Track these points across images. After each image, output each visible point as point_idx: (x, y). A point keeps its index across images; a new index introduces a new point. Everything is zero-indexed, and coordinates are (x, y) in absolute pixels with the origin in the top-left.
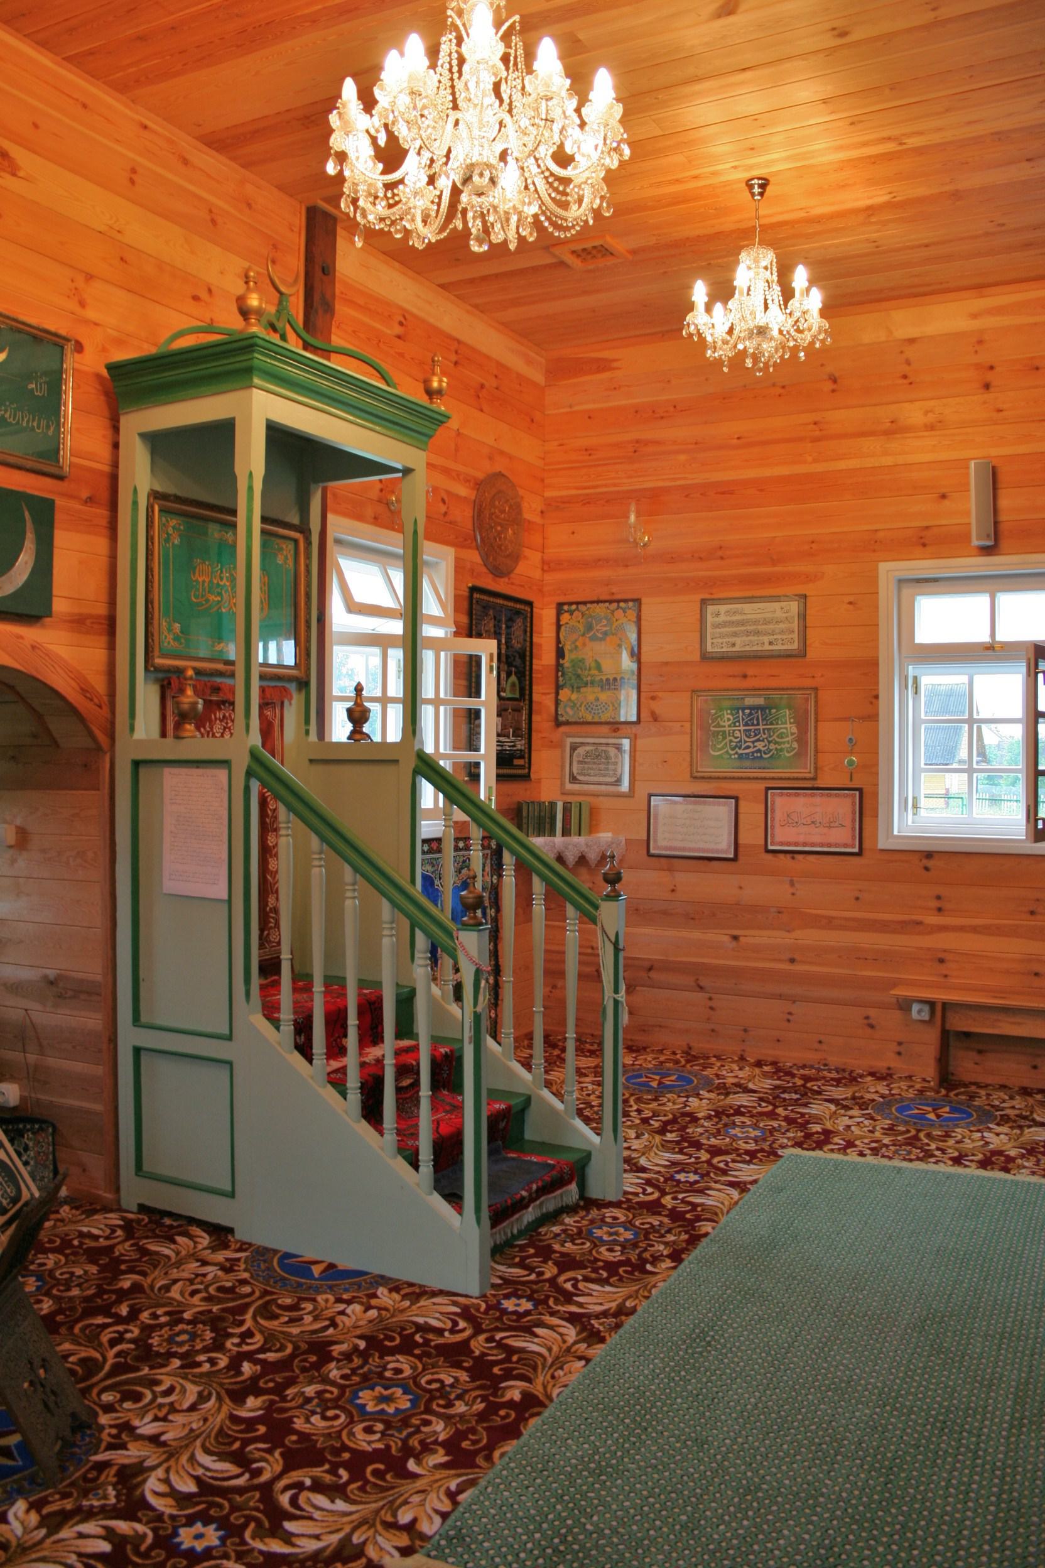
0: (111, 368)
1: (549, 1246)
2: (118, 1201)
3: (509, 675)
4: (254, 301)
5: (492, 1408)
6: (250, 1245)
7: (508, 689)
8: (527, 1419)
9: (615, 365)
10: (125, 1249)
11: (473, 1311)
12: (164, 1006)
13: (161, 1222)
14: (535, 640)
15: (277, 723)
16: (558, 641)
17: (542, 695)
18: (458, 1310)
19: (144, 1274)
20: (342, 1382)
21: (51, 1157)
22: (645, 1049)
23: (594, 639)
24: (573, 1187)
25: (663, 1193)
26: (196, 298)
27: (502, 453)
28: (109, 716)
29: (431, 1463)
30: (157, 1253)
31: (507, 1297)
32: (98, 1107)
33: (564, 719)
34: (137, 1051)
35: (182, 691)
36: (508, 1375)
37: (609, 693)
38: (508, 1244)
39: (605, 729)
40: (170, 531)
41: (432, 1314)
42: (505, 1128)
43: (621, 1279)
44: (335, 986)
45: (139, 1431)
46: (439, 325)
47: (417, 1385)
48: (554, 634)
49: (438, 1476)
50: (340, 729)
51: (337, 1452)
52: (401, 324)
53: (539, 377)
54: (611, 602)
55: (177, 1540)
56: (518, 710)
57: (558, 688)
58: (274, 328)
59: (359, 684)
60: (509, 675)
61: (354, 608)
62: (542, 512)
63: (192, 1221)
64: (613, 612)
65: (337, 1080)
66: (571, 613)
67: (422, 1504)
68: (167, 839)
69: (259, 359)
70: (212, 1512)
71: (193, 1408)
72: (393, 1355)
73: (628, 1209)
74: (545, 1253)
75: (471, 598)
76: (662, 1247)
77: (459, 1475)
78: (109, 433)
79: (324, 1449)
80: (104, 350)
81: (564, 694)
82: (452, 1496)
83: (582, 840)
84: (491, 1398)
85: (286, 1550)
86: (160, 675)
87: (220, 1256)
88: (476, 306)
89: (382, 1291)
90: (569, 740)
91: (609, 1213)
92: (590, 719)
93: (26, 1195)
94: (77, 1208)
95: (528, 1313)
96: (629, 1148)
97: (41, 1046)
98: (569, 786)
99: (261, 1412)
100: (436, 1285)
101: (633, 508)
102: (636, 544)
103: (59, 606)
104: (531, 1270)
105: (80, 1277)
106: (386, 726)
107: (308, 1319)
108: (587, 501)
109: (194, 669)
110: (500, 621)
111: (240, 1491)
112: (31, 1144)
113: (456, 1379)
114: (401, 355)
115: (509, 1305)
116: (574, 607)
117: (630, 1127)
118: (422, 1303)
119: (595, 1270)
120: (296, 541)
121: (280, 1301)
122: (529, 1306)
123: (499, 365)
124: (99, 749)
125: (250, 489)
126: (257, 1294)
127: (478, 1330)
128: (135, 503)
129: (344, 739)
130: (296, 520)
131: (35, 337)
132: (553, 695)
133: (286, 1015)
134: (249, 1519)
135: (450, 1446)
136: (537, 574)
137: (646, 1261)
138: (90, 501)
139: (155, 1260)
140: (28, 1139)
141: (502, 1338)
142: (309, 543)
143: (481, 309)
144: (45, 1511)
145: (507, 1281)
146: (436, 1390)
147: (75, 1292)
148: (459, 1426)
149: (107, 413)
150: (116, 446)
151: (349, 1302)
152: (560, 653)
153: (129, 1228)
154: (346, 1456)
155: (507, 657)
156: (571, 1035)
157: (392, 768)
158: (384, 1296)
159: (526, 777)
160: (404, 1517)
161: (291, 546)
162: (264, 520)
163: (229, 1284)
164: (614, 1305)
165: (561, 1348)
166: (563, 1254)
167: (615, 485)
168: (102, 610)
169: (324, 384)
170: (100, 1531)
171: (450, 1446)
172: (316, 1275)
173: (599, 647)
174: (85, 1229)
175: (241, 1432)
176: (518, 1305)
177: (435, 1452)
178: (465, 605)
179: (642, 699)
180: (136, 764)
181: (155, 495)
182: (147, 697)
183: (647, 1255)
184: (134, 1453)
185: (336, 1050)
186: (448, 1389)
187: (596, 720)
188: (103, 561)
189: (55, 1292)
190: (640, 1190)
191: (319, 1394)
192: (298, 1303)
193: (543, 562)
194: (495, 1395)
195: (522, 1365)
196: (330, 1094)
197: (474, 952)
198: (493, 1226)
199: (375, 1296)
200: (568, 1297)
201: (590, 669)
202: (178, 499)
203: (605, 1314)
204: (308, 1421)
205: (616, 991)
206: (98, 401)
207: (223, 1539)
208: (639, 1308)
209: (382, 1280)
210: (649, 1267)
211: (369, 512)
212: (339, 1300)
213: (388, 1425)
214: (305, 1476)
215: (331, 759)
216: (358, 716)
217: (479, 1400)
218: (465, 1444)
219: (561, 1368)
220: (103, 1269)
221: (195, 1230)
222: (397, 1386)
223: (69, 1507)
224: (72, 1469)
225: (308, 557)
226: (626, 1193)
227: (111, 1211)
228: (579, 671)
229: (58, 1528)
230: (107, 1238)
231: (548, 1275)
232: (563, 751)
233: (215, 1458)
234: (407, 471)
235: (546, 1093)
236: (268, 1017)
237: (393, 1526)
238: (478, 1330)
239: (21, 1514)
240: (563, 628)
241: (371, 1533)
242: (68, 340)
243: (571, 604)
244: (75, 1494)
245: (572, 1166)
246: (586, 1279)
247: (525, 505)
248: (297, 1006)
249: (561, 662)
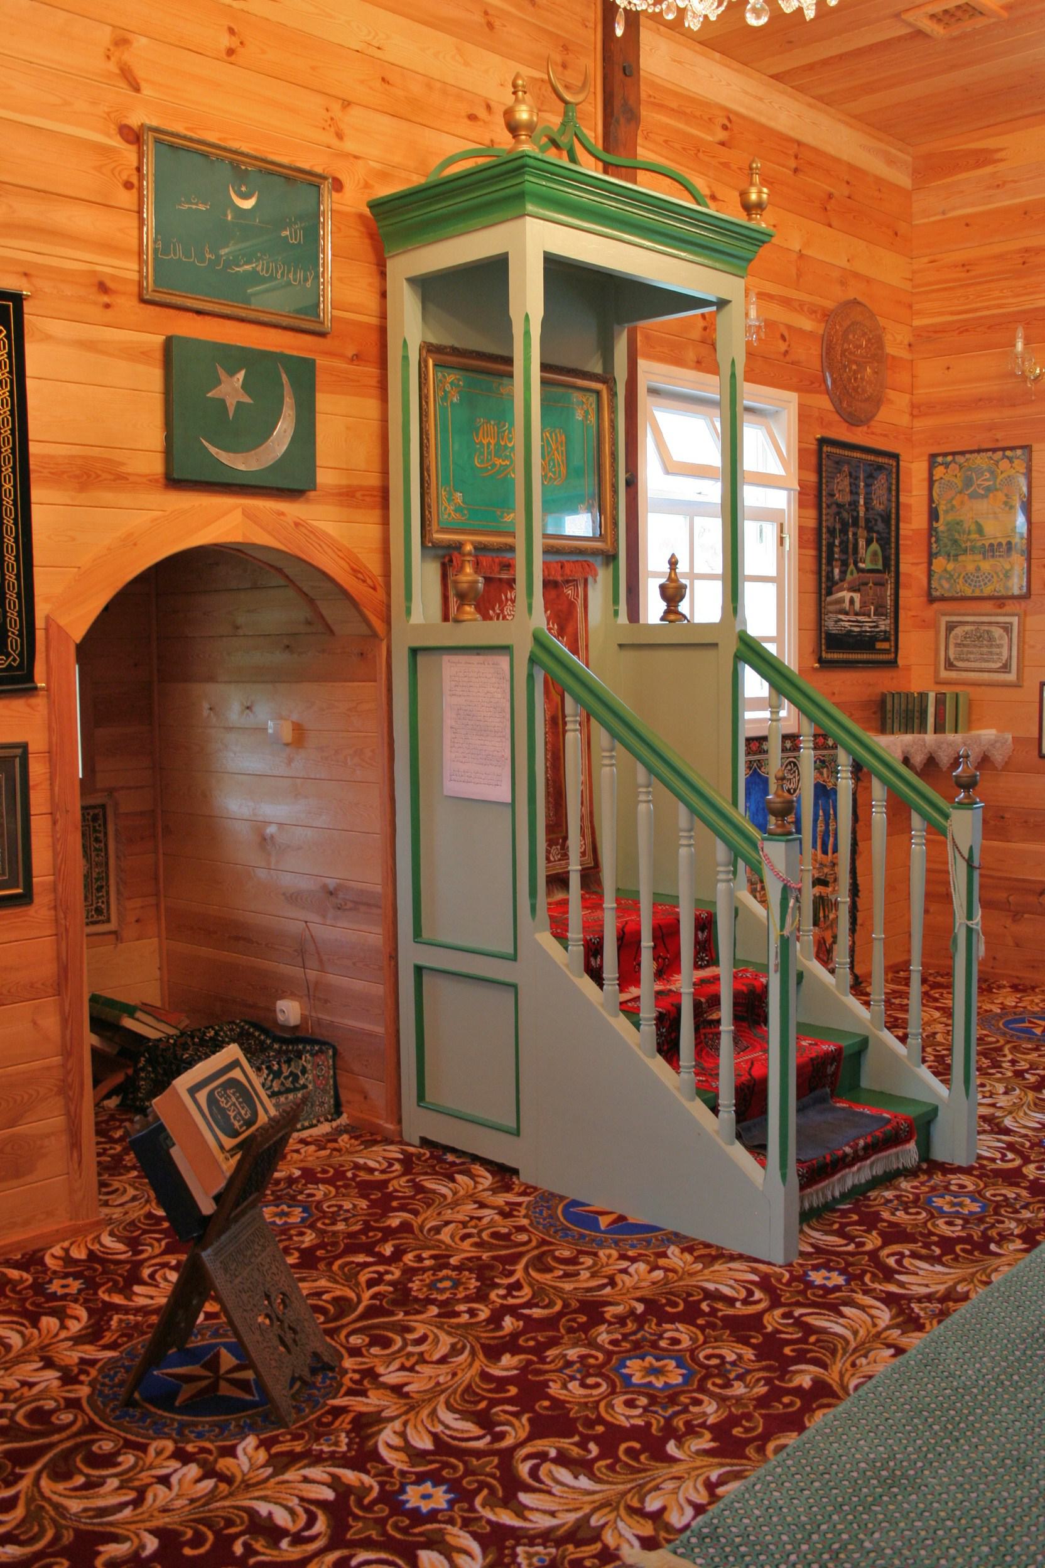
0: (374, 205)
1: (877, 1214)
2: (401, 1136)
3: (869, 542)
4: (523, 114)
5: (775, 1393)
6: (535, 1189)
7: (868, 560)
8: (814, 1411)
9: (998, 156)
10: (400, 1185)
11: (773, 1281)
12: (445, 924)
13: (442, 1158)
14: (902, 499)
15: (580, 602)
16: (931, 500)
17: (911, 564)
18: (756, 1278)
19: (416, 1213)
20: (610, 1347)
21: (331, 1082)
22: (1033, 988)
23: (972, 497)
24: (912, 1146)
25: (1027, 1161)
26: (472, 117)
27: (856, 275)
28: (384, 598)
29: (693, 1448)
30: (434, 1191)
31: (816, 1268)
32: (379, 1029)
33: (938, 594)
34: (419, 970)
35: (461, 569)
36: (801, 1357)
37: (992, 561)
38: (829, 1207)
39: (988, 606)
40: (448, 388)
41: (725, 1280)
42: (835, 1074)
43: (956, 1259)
44: (628, 905)
45: (382, 1379)
46: (772, 124)
47: (694, 1358)
48: (925, 492)
49: (698, 1463)
50: (654, 609)
51: (590, 1423)
52: (725, 127)
53: (904, 180)
54: (994, 450)
55: (403, 1497)
56: (882, 584)
57: (931, 556)
58: (554, 143)
59: (673, 556)
60: (869, 542)
61: (671, 468)
62: (910, 345)
63: (475, 1159)
64: (997, 463)
65: (630, 1010)
66: (947, 465)
67: (675, 1491)
68: (448, 736)
69: (531, 182)
70: (444, 1473)
71: (443, 1360)
72: (673, 1323)
73: (979, 1177)
74: (871, 1221)
75: (820, 451)
76: (1013, 1225)
77: (722, 1465)
78: (376, 280)
79: (577, 1419)
80: (367, 186)
81: (939, 563)
82: (710, 1487)
83: (957, 738)
84: (777, 1382)
85: (517, 1523)
86: (441, 552)
87: (500, 1199)
88: (820, 98)
89: (673, 1250)
90: (944, 620)
91: (955, 1180)
92: (968, 592)
93: (262, 1119)
94: (356, 1138)
95: (837, 1288)
96: (993, 1105)
97: (321, 961)
98: (944, 674)
99: (516, 1372)
100: (734, 1246)
101: (1020, 333)
102: (1024, 378)
103: (325, 477)
104: (850, 1239)
105: (348, 1211)
106: (704, 606)
107: (584, 1275)
108: (963, 329)
109: (472, 543)
110: (857, 478)
111: (478, 1454)
112: (309, 1067)
113: (740, 1357)
114: (726, 165)
115: (817, 1277)
116: (949, 458)
117: (999, 1080)
118: (716, 1267)
119: (927, 1246)
120: (598, 393)
121: (557, 1253)
122: (840, 1280)
123: (853, 168)
124: (375, 635)
125: (527, 334)
126: (534, 1243)
127: (775, 1303)
128: (405, 358)
129: (658, 621)
130: (598, 369)
131: (287, 178)
132: (925, 565)
133: (575, 933)
134: (482, 1485)
135: (720, 1431)
136: (904, 420)
137: (991, 1240)
138: (357, 358)
139: (429, 1198)
140: (306, 1060)
141: (802, 1315)
142: (613, 394)
143: (826, 101)
144: (274, 1450)
145: (819, 1250)
146: (716, 1366)
147: (341, 1226)
148: (733, 1409)
149: (371, 257)
150: (384, 295)
151: (633, 1260)
152: (933, 515)
153: (408, 1162)
154: (600, 1429)
155: (867, 521)
156: (916, 967)
157: (710, 654)
158: (675, 1257)
159: (893, 664)
160: (653, 1504)
161: (593, 398)
162: (544, 367)
163: (505, 1230)
164: (942, 1288)
165: (869, 1332)
166: (891, 1224)
167: (1000, 306)
168: (374, 480)
169: (612, 206)
170: (326, 1478)
171: (720, 1431)
172: (603, 1228)
173: (982, 506)
174: (361, 1161)
175: (490, 1391)
176: (828, 1278)
177: (699, 1435)
178: (813, 460)
179: (1034, 568)
180: (414, 652)
181: (428, 349)
182: (425, 578)
183: (993, 1233)
184: (374, 1400)
185: (629, 976)
186: (728, 1367)
187: (977, 594)
188: (375, 426)
189: (319, 1225)
190: (999, 1156)
191: (583, 1358)
192: (577, 1257)
193: (913, 406)
194: (781, 1378)
195: (816, 1347)
196: (621, 1023)
197: (781, 867)
198: (802, 1188)
199: (664, 1255)
200: (888, 1274)
201: (969, 533)
202: (455, 351)
203: (929, 1298)
204: (564, 1386)
205: (970, 917)
206: (363, 246)
207: (451, 1503)
208: (973, 1295)
209: (675, 1238)
210: (993, 1247)
211: (691, 355)
212: (623, 1257)
213: (653, 1400)
214: (550, 1446)
215: (643, 645)
216: (673, 593)
217: (762, 1382)
218: (737, 1431)
219: (866, 1356)
220: (373, 1204)
221: (478, 1169)
222: (671, 1358)
223: (298, 1449)
224: (307, 1410)
225: (613, 410)
226: (980, 1157)
227: (392, 1143)
228: (957, 536)
229: (285, 1468)
230: (383, 1172)
231: (869, 1247)
232: (937, 633)
233: (457, 1416)
234: (722, 304)
235: (889, 1038)
236: (556, 936)
237: (638, 1512)
238: (775, 1303)
239: (250, 1450)
241: (612, 1516)
242: (325, 178)
243: (945, 455)
244: (307, 1437)
245: (911, 1122)
246: (914, 1255)
247: (888, 338)
248: (586, 926)
249: (935, 525)
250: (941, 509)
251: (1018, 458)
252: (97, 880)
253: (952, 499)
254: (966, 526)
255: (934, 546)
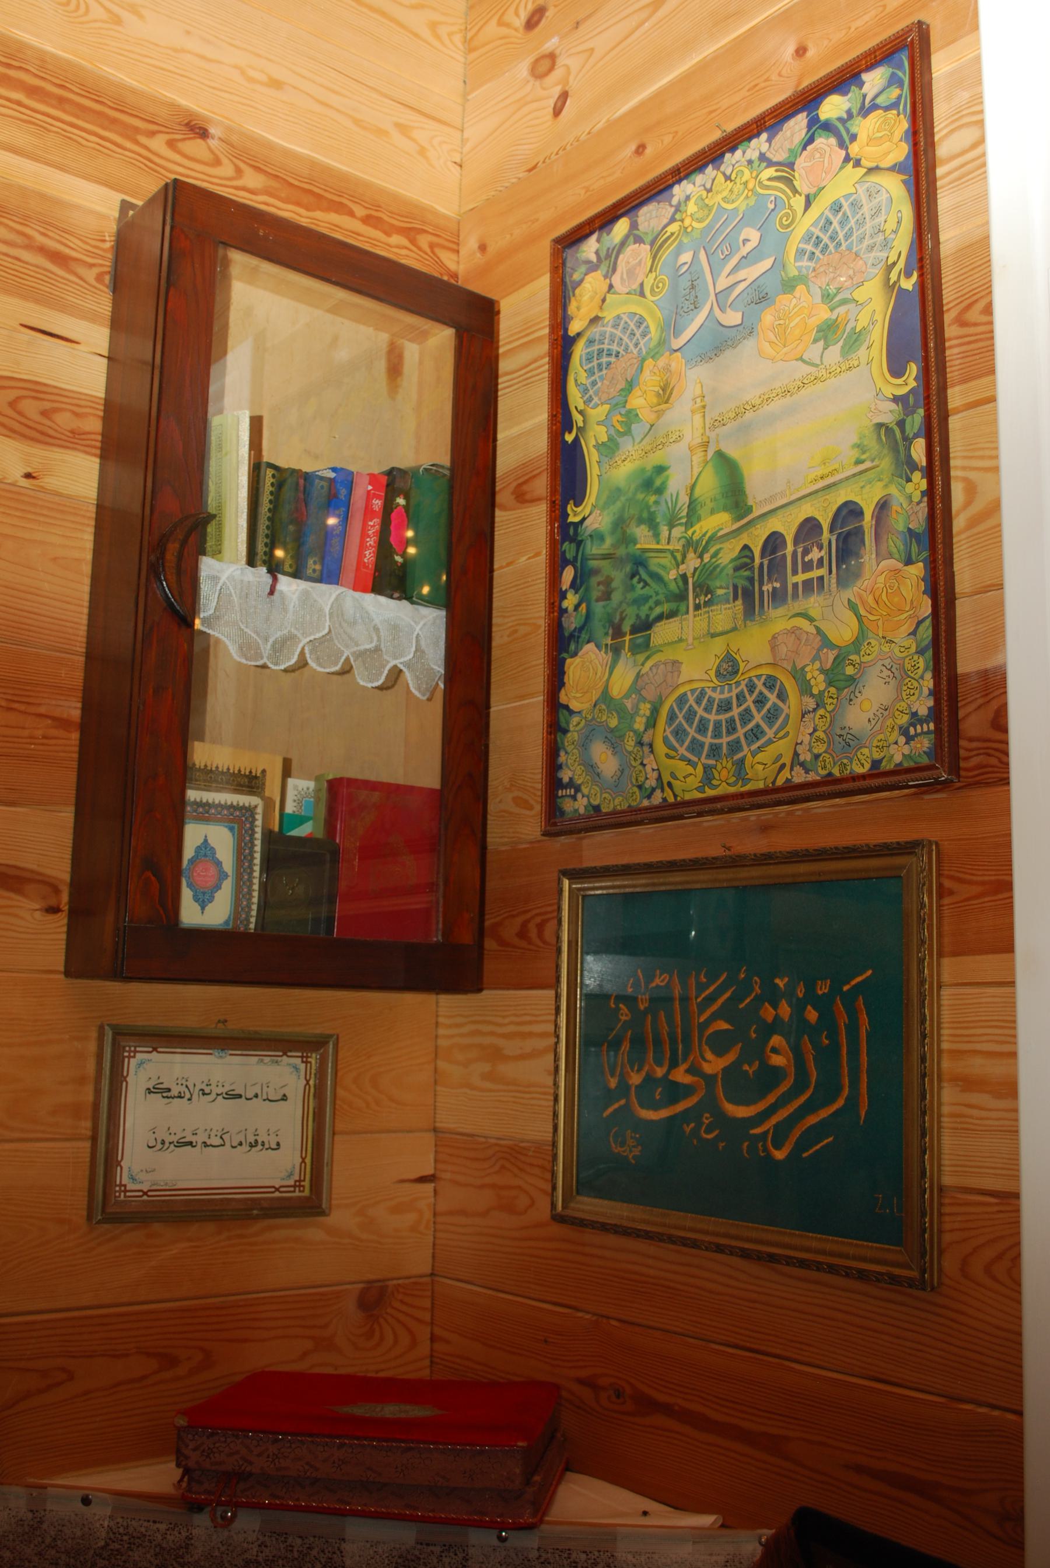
33: (581, 805)
66: (609, 259)
116: (622, 227)
240: (579, 351)
250: (593, 437)
251: (866, 110)
253: (630, 385)
254: (676, 483)
255: (570, 601)
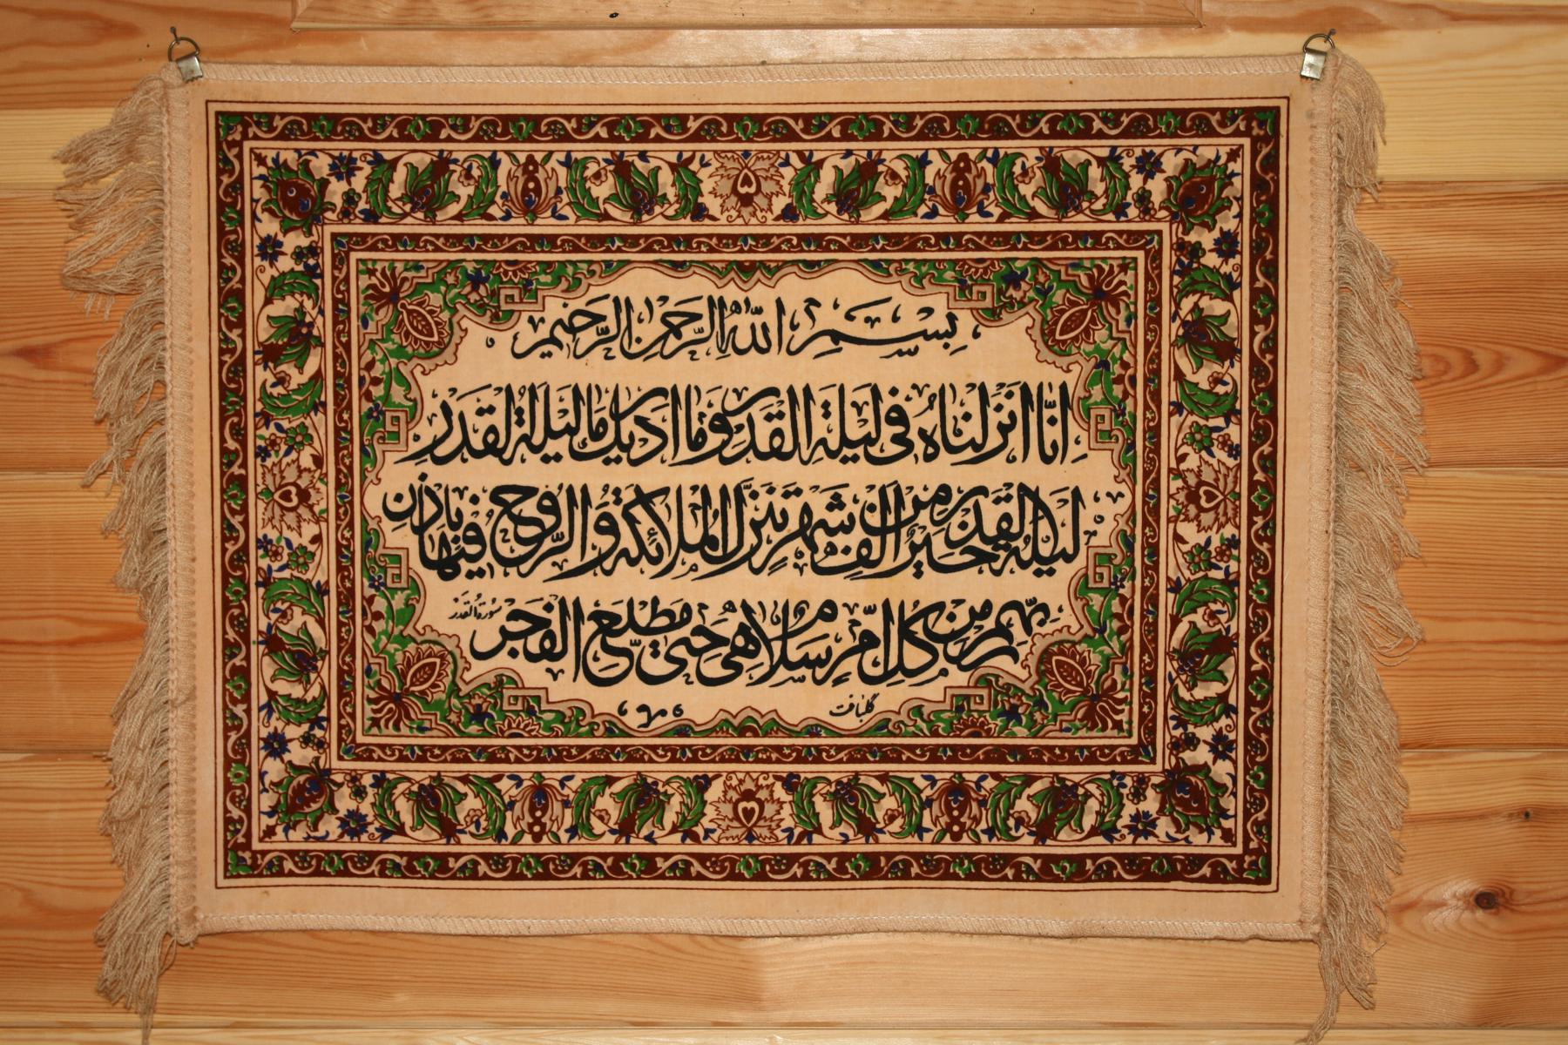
252: (1189, 596)
